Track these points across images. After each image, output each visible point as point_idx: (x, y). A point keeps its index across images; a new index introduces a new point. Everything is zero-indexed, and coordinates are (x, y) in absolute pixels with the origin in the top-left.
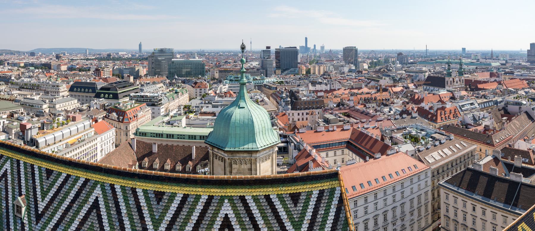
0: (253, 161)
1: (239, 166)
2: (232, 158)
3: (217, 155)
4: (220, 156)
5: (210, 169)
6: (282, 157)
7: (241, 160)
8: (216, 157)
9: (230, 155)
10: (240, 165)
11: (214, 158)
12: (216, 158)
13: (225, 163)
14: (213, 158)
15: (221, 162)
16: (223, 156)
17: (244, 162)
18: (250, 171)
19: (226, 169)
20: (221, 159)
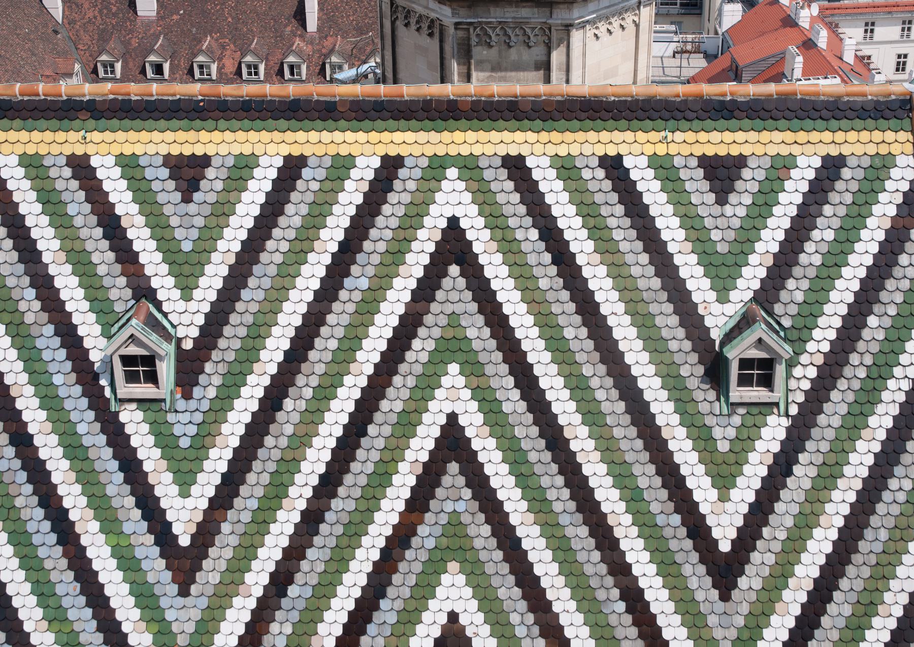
0: (555, 36)
1: (500, 52)
2: (471, 24)
3: (408, 13)
4: (420, 16)
5: (383, 64)
6: (673, 28)
7: (509, 31)
8: (406, 17)
9: (463, 12)
10: (504, 47)
11: (399, 24)
12: (407, 25)
13: (441, 41)
14: (393, 23)
15: (428, 39)
16: (433, 15)
17: (521, 38)
18: (547, 72)
19: (447, 62)
20: (425, 25)
